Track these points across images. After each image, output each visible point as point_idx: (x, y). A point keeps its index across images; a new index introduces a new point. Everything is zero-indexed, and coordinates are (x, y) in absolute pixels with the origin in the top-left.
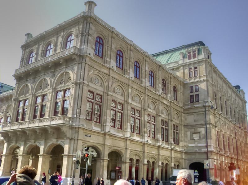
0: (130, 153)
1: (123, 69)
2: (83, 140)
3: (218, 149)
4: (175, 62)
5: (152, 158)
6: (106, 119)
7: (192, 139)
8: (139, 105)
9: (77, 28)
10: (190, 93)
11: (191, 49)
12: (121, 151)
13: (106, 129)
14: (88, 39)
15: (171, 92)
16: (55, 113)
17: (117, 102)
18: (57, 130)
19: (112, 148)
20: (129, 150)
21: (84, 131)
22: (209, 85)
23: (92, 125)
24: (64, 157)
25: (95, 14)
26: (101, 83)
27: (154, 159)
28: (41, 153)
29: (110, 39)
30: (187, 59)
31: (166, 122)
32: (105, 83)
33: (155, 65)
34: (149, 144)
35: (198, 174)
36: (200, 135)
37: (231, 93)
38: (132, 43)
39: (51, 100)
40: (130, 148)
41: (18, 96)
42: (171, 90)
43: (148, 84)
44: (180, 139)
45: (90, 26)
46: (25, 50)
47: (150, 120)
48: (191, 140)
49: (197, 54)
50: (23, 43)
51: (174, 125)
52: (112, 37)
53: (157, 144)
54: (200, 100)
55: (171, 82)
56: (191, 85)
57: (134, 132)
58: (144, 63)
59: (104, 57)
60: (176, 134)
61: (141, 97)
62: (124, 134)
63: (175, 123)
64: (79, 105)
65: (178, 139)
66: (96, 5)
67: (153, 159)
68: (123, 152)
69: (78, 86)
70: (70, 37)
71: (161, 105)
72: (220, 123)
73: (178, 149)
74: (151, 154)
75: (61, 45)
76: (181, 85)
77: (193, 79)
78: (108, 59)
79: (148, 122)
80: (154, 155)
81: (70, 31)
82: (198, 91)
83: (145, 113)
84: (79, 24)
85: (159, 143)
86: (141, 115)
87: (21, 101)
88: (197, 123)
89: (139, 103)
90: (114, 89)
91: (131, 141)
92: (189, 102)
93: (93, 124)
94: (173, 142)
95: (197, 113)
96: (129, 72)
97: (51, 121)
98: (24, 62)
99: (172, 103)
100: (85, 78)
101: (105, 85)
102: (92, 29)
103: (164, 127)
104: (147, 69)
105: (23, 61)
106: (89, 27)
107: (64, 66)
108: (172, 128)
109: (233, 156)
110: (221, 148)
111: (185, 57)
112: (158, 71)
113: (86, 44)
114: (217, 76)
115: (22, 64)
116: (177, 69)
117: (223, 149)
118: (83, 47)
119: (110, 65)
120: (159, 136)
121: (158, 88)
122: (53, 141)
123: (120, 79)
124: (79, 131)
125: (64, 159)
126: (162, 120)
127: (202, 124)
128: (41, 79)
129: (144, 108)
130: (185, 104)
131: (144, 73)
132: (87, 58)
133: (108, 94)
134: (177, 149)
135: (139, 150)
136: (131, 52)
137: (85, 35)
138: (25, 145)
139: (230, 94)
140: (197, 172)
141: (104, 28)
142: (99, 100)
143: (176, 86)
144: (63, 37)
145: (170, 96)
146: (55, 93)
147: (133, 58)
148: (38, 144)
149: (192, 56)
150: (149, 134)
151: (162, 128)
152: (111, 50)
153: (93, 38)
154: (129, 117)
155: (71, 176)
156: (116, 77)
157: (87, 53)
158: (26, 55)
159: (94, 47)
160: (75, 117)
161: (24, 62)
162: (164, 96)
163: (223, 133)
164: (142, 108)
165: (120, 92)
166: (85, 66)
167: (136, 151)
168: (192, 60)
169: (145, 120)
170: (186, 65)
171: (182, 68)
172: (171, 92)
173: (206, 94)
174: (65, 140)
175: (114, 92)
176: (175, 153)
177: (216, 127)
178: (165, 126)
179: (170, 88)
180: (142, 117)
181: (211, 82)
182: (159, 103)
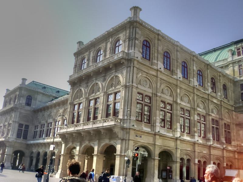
0: (180, 153)
2: (134, 140)
4: (224, 60)
5: (202, 157)
8: (189, 105)
9: (124, 33)
10: (241, 90)
11: (240, 45)
12: (172, 150)
13: (156, 130)
14: (135, 43)
15: (220, 91)
16: (108, 115)
17: (166, 103)
18: (110, 131)
19: (162, 148)
21: (135, 132)
23: (142, 125)
24: (116, 156)
25: (140, 18)
26: (150, 85)
27: (206, 158)
29: (156, 41)
30: (237, 56)
31: (217, 121)
33: (203, 64)
38: (178, 44)
39: (103, 103)
40: (180, 147)
42: (220, 88)
43: (196, 83)
44: (233, 138)
45: (137, 31)
46: (77, 57)
50: (75, 50)
51: (225, 124)
52: (158, 40)
53: (208, 143)
55: (220, 80)
57: (184, 132)
59: (151, 60)
61: (189, 96)
62: (174, 134)
64: (129, 107)
66: (141, 10)
68: (174, 151)
70: (118, 42)
73: (230, 148)
74: (202, 154)
76: (231, 83)
78: (156, 61)
79: (198, 122)
80: (205, 155)
81: (118, 36)
83: (194, 112)
85: (210, 142)
86: (191, 115)
87: (76, 104)
91: (181, 141)
92: (241, 100)
93: (143, 125)
94: (224, 142)
96: (176, 72)
97: (103, 123)
98: (77, 68)
99: (222, 102)
100: (134, 81)
101: (154, 87)
102: (138, 33)
104: (195, 68)
105: (76, 67)
106: (136, 31)
107: (113, 70)
108: (223, 127)
111: (235, 54)
112: (206, 70)
113: (133, 48)
116: (227, 66)
118: (130, 51)
119: (157, 67)
120: (210, 136)
121: (207, 87)
122: (106, 142)
123: (168, 80)
124: (129, 132)
125: (116, 158)
129: (193, 108)
131: (192, 73)
132: (135, 62)
133: (157, 95)
136: (178, 53)
137: (132, 40)
138: (80, 146)
141: (150, 31)
142: (149, 102)
144: (111, 43)
146: (106, 96)
147: (180, 59)
148: (92, 145)
150: (199, 134)
151: (213, 127)
152: (158, 52)
153: (140, 42)
154: (178, 118)
155: (123, 174)
157: (134, 56)
158: (79, 62)
159: (141, 51)
160: (126, 118)
161: (77, 68)
162: (214, 95)
164: (191, 108)
165: (168, 93)
166: (133, 70)
167: (186, 151)
169: (194, 120)
170: (235, 62)
171: (231, 65)
172: (220, 91)
174: (117, 140)
175: (162, 92)
176: (227, 153)
178: (216, 125)
179: (220, 86)
182: (209, 101)
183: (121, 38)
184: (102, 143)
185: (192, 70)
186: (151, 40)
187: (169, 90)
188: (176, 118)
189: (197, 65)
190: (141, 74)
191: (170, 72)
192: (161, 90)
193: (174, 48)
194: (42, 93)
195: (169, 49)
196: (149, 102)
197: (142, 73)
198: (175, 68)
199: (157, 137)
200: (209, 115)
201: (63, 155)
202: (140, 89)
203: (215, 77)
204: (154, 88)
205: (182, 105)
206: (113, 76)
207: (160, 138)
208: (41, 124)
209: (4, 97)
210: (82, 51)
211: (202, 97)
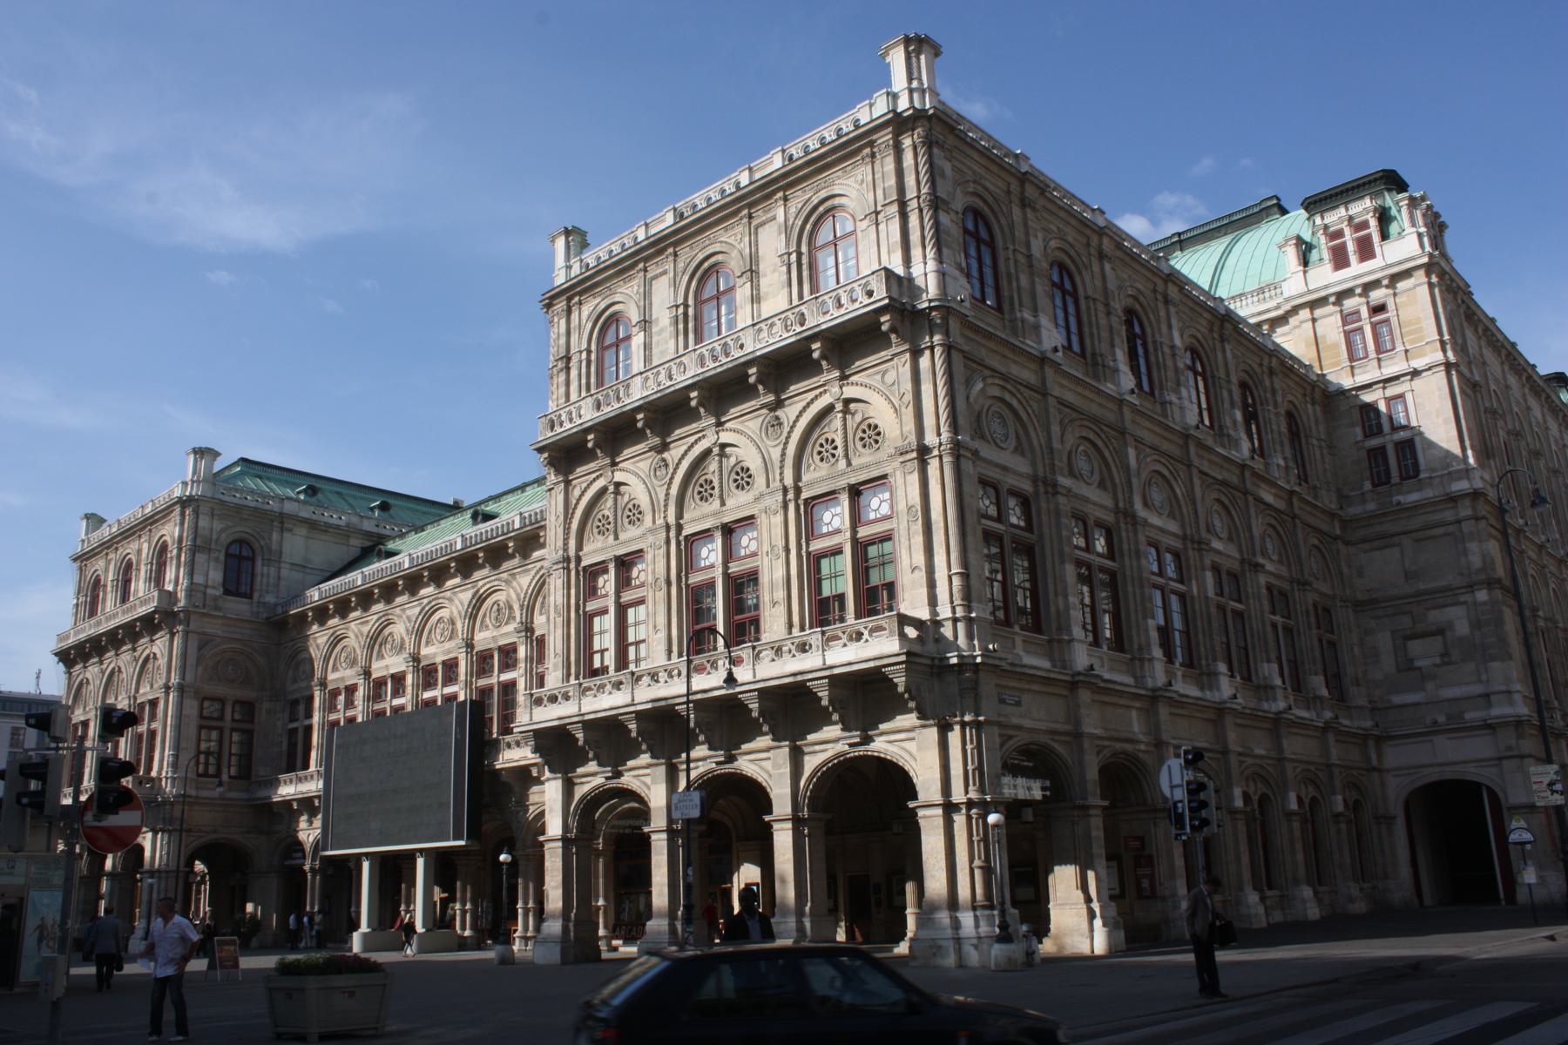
1: (1088, 355)
4: (1261, 290)
6: (1067, 609)
9: (864, 172)
10: (1366, 436)
11: (1342, 211)
15: (1282, 446)
16: (824, 611)
17: (1091, 522)
19: (1104, 747)
26: (1018, 437)
27: (1266, 782)
29: (1017, 212)
30: (1328, 266)
32: (1033, 435)
33: (1206, 315)
40: (1174, 738)
41: (572, 543)
42: (1280, 432)
49: (1376, 238)
52: (1024, 204)
53: (1265, 706)
54: (1422, 467)
55: (1274, 392)
58: (1162, 314)
59: (1006, 307)
75: (784, 269)
76: (1313, 403)
77: (1375, 363)
78: (1027, 315)
84: (873, 155)
85: (1275, 699)
88: (1422, 586)
89: (1171, 515)
91: (1171, 706)
92: (1368, 486)
93: (1018, 641)
95: (1415, 535)
96: (1111, 363)
101: (1035, 442)
102: (943, 175)
103: (1278, 618)
112: (1218, 345)
114: (1479, 338)
119: (1040, 342)
120: (1270, 671)
121: (1231, 432)
124: (977, 682)
127: (1449, 588)
129: (1196, 538)
130: (1348, 496)
131: (1169, 363)
133: (1055, 485)
134: (1345, 722)
136: (1107, 267)
140: (1522, 824)
141: (986, 163)
143: (1296, 414)
145: (1281, 462)
149: (1351, 247)
151: (1274, 625)
152: (1031, 266)
154: (1147, 590)
161: (574, 373)
164: (1184, 538)
175: (1072, 474)
178: (1283, 617)
180: (1194, 582)
185: (1166, 350)
186: (996, 207)
191: (1086, 364)
193: (1085, 241)
194: (305, 521)
195: (1067, 248)
196: (1022, 524)
197: (984, 379)
198: (1102, 344)
199: (1085, 695)
200: (1257, 567)
202: (990, 463)
204: (1038, 453)
205: (1152, 526)
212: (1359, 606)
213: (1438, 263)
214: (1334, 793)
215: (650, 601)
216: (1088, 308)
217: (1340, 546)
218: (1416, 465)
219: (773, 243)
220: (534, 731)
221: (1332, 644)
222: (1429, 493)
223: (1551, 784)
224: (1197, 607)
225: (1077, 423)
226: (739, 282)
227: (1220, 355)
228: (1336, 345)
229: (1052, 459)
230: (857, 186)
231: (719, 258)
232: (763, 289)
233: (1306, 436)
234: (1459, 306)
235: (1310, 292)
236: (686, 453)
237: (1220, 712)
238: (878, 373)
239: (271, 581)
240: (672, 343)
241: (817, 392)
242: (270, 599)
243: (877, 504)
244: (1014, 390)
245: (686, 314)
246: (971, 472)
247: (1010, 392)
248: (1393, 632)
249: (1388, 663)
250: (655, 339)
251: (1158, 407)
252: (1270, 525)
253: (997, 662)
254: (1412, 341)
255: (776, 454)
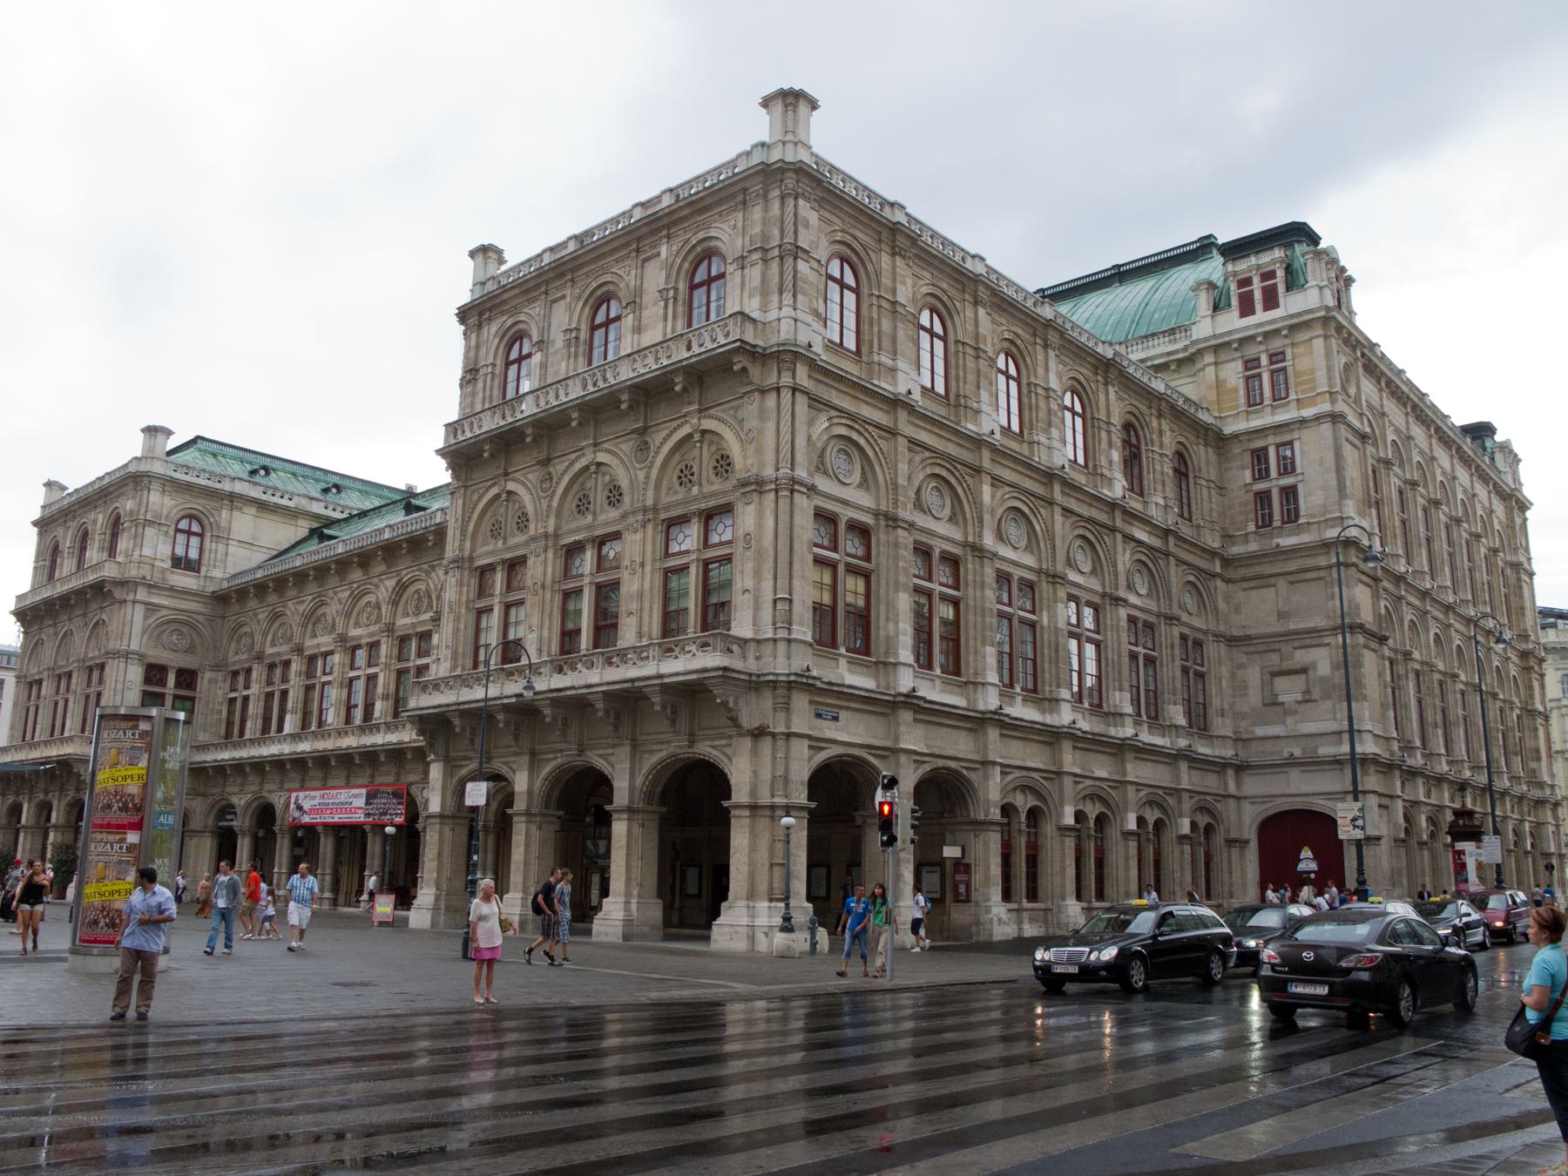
2: (809, 737)
3: (1395, 746)
4: (1172, 331)
6: (897, 634)
7: (1273, 703)
8: (1029, 560)
10: (1254, 479)
11: (1253, 260)
14: (795, 272)
16: (671, 623)
17: (936, 554)
20: (998, 769)
22: (1347, 440)
24: (733, 812)
25: (815, 150)
28: (621, 796)
31: (1149, 626)
34: (1080, 734)
35: (1313, 866)
36: (1307, 680)
37: (1452, 465)
38: (979, 269)
40: (1001, 757)
42: (1162, 473)
44: (1216, 702)
46: (480, 326)
47: (1078, 626)
48: (1265, 705)
50: (465, 298)
51: (1183, 637)
55: (1161, 433)
56: (1259, 444)
57: (1011, 686)
58: (1040, 357)
59: (864, 350)
60: (1195, 677)
61: (1032, 518)
63: (1186, 631)
64: (782, 581)
65: (1204, 705)
66: (814, 105)
67: (1097, 805)
69: (772, 496)
71: (1124, 550)
72: (1401, 620)
73: (1203, 749)
74: (1088, 782)
75: (662, 303)
76: (1206, 445)
79: (1072, 635)
80: (1104, 784)
82: (1294, 469)
84: (744, 203)
86: (1041, 601)
87: (491, 568)
88: (1292, 626)
90: (918, 491)
91: (1002, 727)
92: (1252, 527)
93: (843, 662)
94: (1181, 721)
95: (1291, 578)
96: (975, 405)
100: (799, 457)
102: (807, 226)
103: (1140, 649)
106: (796, 214)
107: (690, 403)
108: (1177, 652)
109: (1467, 774)
110: (1409, 742)
112: (1101, 388)
114: (1381, 390)
115: (473, 395)
116: (1186, 362)
117: (1418, 743)
119: (895, 384)
122: (665, 747)
125: (733, 821)
126: (1132, 620)
128: (578, 466)
130: (1230, 537)
131: (1042, 404)
132: (798, 365)
134: (1202, 750)
135: (1041, 766)
138: (533, 768)
139: (1444, 473)
145: (1161, 501)
147: (989, 340)
148: (600, 763)
149: (1258, 295)
151: (1133, 656)
153: (815, 265)
155: (771, 890)
156: (924, 437)
158: (487, 353)
160: (770, 635)
163: (1417, 667)
166: (793, 404)
167: (1024, 773)
168: (1260, 316)
169: (1057, 629)
170: (1228, 344)
171: (1209, 358)
173: (1334, 482)
175: (919, 505)
176: (1193, 772)
177: (1382, 640)
178: (1145, 648)
180: (1045, 613)
181: (1357, 424)
183: (718, 243)
184: (651, 752)
187: (946, 491)
188: (979, 619)
189: (1061, 366)
190: (827, 424)
192: (912, 495)
195: (939, 293)
196: (860, 552)
198: (967, 387)
201: (441, 816)
203: (1137, 419)
205: (1004, 559)
206: (686, 430)
207: (916, 720)
208: (268, 661)
209: (35, 524)
210: (505, 296)
211: (1090, 520)
212: (1232, 641)
213: (1334, 317)
214: (1181, 816)
215: (528, 605)
216: (957, 352)
217: (1219, 583)
218: (1297, 510)
219: (655, 278)
220: (420, 716)
221: (1201, 676)
222: (1305, 538)
223: (1354, 820)
224: (1046, 637)
225: (929, 461)
226: (625, 312)
227: (1102, 397)
228: (1236, 390)
229: (897, 494)
230: (730, 231)
231: (611, 287)
232: (644, 321)
233: (1195, 477)
234: (1356, 359)
235: (1215, 336)
236: (568, 468)
237: (1052, 737)
238: (731, 408)
239: (219, 556)
240: (564, 364)
241: (679, 422)
242: (217, 573)
243: (722, 532)
244: (861, 430)
245: (577, 338)
246: (805, 505)
247: (857, 431)
248: (1262, 668)
249: (1254, 698)
250: (550, 359)
251: (1025, 446)
252: (1139, 561)
253: (811, 681)
254: (1304, 392)
255: (641, 475)
